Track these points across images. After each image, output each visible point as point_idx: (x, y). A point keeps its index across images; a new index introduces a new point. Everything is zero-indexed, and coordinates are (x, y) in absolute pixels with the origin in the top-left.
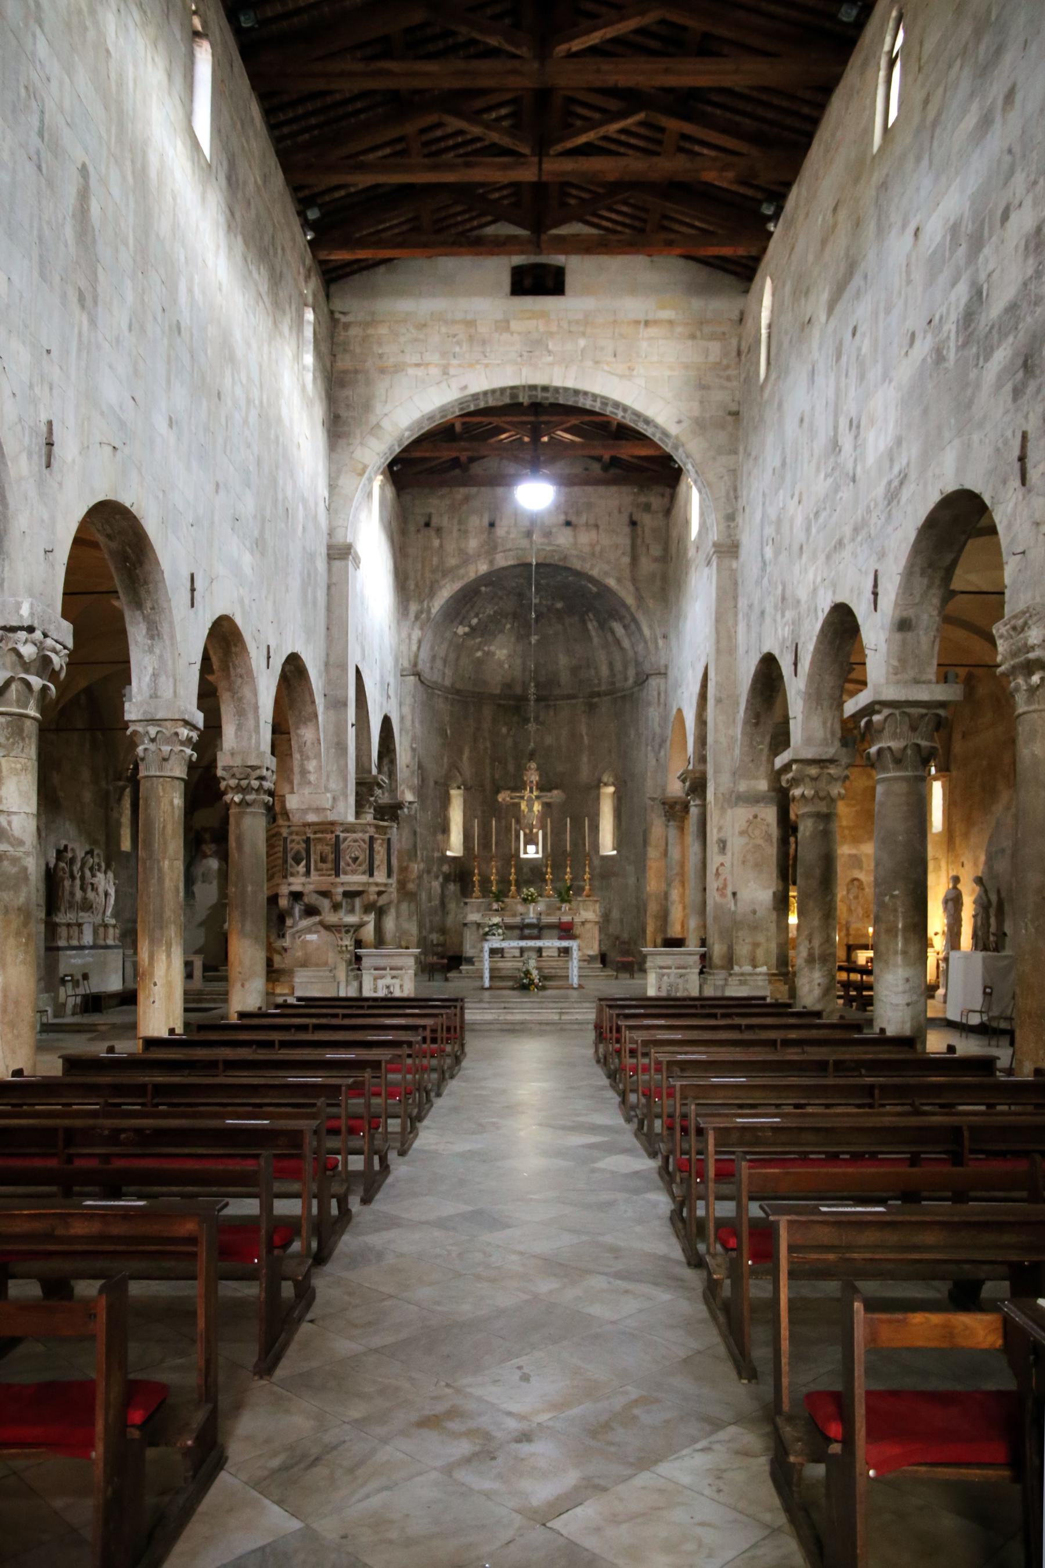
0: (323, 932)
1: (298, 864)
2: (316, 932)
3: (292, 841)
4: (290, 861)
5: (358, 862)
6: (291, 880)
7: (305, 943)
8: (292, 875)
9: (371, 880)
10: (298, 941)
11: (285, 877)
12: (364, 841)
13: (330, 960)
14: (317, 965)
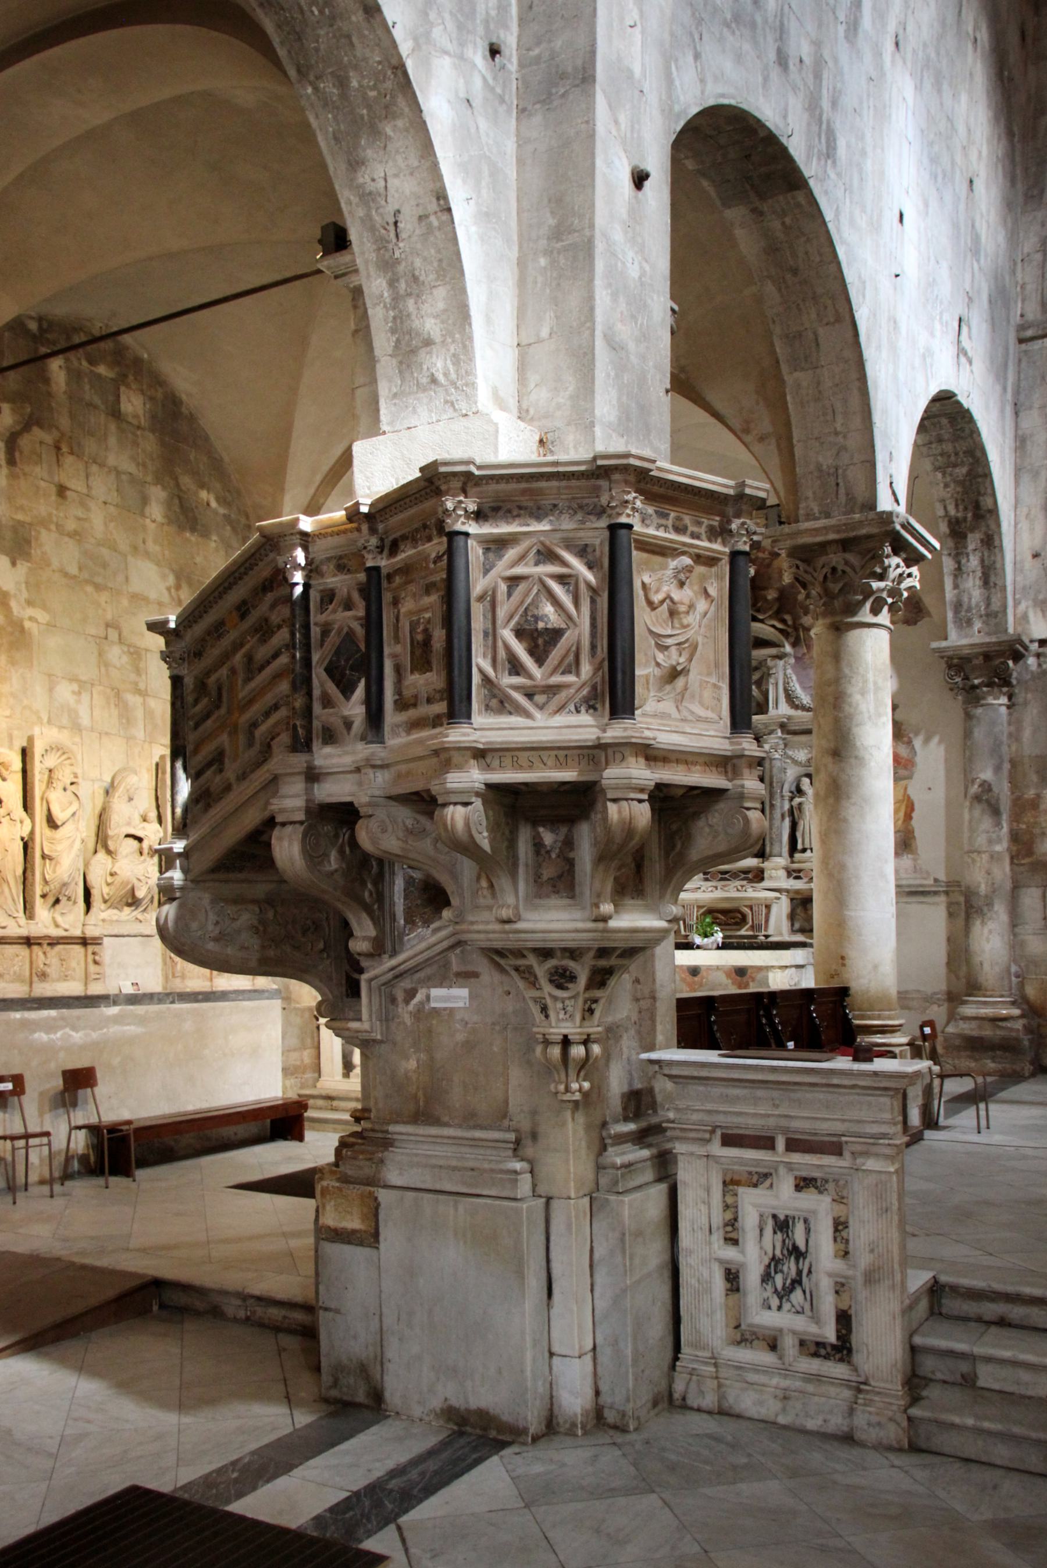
0: (488, 975)
1: (347, 690)
2: (467, 976)
3: (329, 597)
4: (320, 678)
5: (555, 655)
6: (325, 756)
7: (425, 1015)
8: (330, 737)
9: (617, 731)
10: (405, 1012)
11: (302, 744)
12: (582, 552)
13: (518, 1101)
14: (470, 1119)
